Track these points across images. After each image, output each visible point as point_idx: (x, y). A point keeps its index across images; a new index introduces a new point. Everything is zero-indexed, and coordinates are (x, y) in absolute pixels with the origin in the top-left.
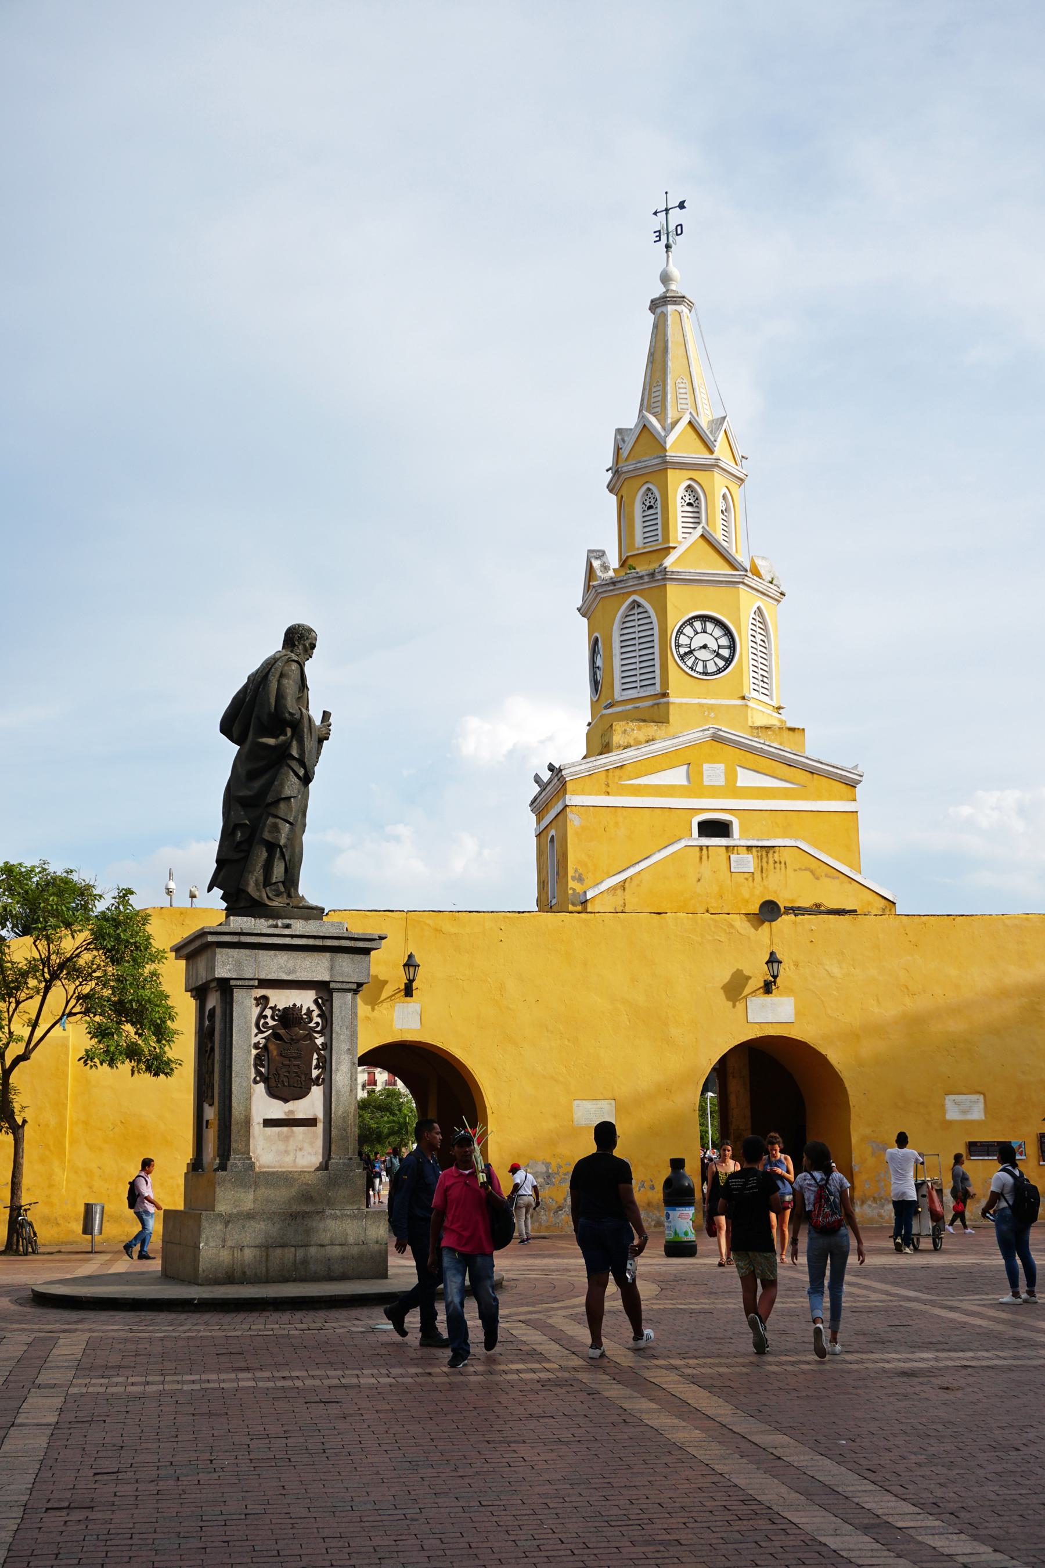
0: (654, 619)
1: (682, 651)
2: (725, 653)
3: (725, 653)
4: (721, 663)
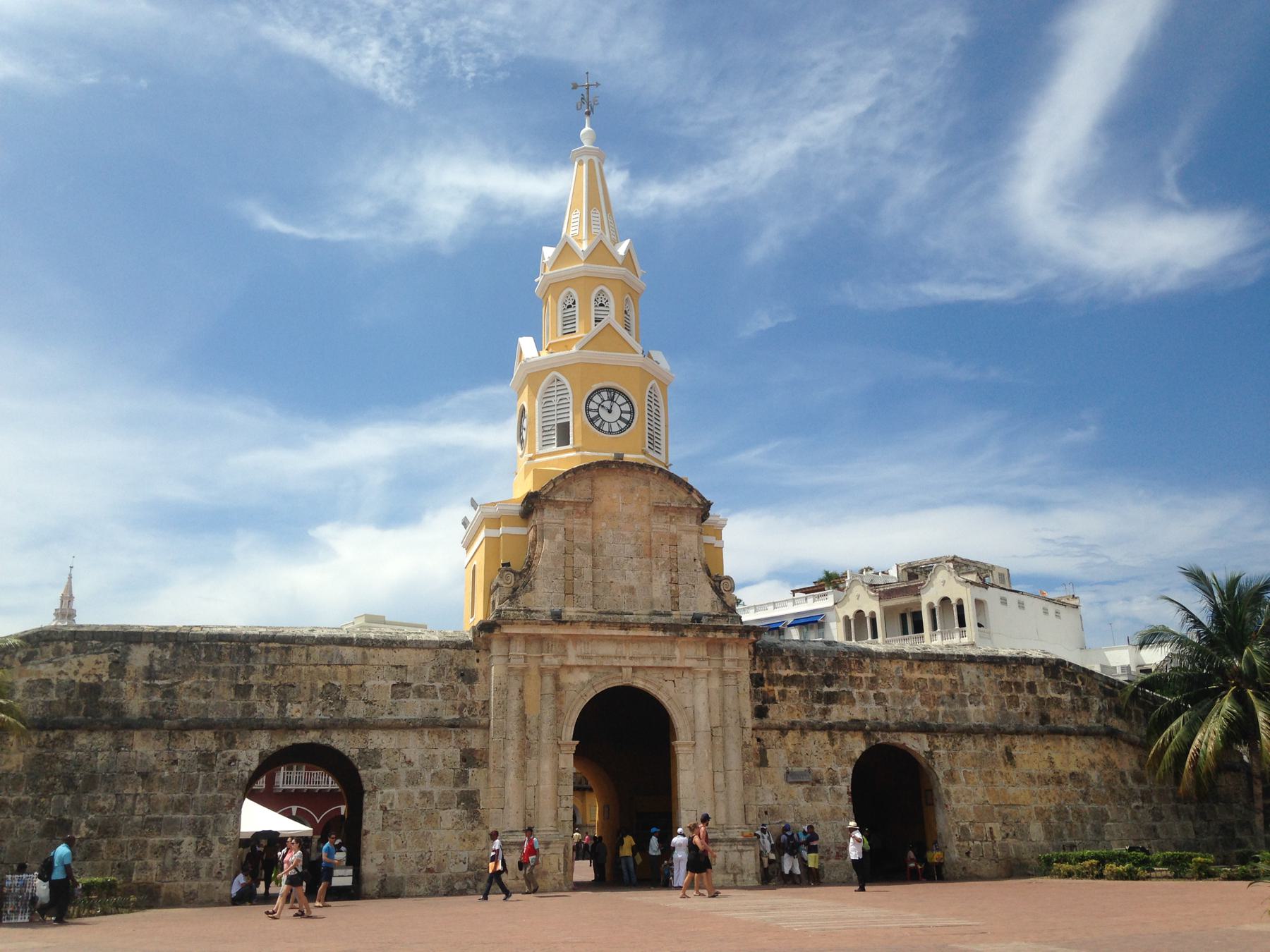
0: (569, 391)
1: (593, 415)
2: (627, 417)
3: (627, 417)
4: (623, 425)
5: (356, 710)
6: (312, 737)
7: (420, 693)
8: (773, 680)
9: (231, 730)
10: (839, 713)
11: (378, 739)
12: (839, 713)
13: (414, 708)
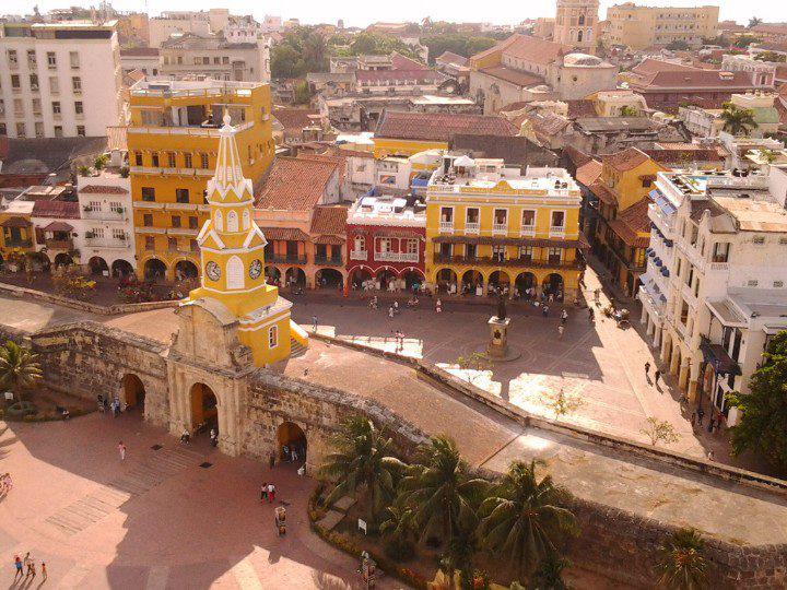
5: (143, 369)
6: (133, 372)
7: (156, 367)
8: (254, 391)
9: (117, 366)
10: (275, 408)
11: (148, 378)
12: (275, 408)
13: (155, 371)
